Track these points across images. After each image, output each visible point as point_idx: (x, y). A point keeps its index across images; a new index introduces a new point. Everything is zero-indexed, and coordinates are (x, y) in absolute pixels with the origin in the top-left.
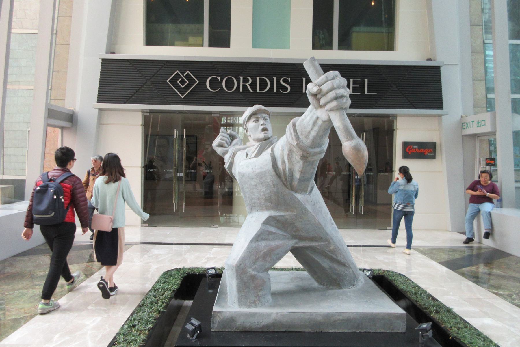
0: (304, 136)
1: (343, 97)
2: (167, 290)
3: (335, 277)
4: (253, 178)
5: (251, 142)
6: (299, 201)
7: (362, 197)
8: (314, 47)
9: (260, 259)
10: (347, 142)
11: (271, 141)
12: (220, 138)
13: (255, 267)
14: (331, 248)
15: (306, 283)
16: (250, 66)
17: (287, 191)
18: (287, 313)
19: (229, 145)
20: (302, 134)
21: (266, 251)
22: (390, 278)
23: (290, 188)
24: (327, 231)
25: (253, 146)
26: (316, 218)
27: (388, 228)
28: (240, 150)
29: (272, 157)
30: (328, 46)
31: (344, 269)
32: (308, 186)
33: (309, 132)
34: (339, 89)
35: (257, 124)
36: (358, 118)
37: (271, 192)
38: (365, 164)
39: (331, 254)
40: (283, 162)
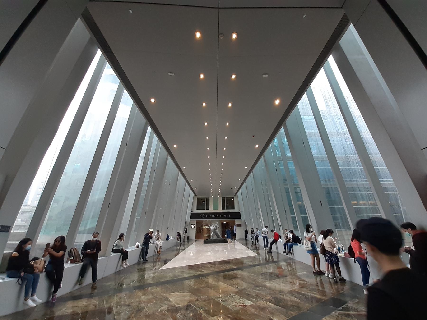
8: (222, 209)
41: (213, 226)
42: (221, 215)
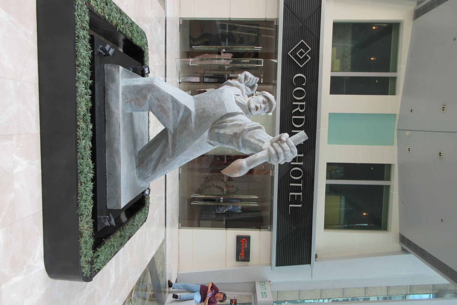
0: (251, 134)
1: (278, 159)
2: (132, 34)
3: (145, 162)
4: (220, 99)
5: (248, 99)
6: (203, 133)
7: (205, 203)
9: (159, 103)
10: (245, 162)
11: (248, 113)
12: (252, 77)
13: (153, 99)
14: (167, 159)
15: (139, 142)
16: (314, 111)
17: (210, 124)
18: (119, 121)
19: (246, 84)
20: (252, 133)
21: (165, 108)
22: (144, 210)
23: (213, 127)
24: (180, 156)
25: (245, 100)
26: (190, 147)
27: (180, 224)
28: (242, 92)
29: (236, 113)
30: (330, 176)
31: (151, 169)
32: (214, 140)
33: (253, 138)
34: (284, 156)
35: (261, 102)
36: (270, 200)
37: (209, 112)
38: (230, 174)
39: (162, 159)
40: (232, 121)
41: (248, 110)
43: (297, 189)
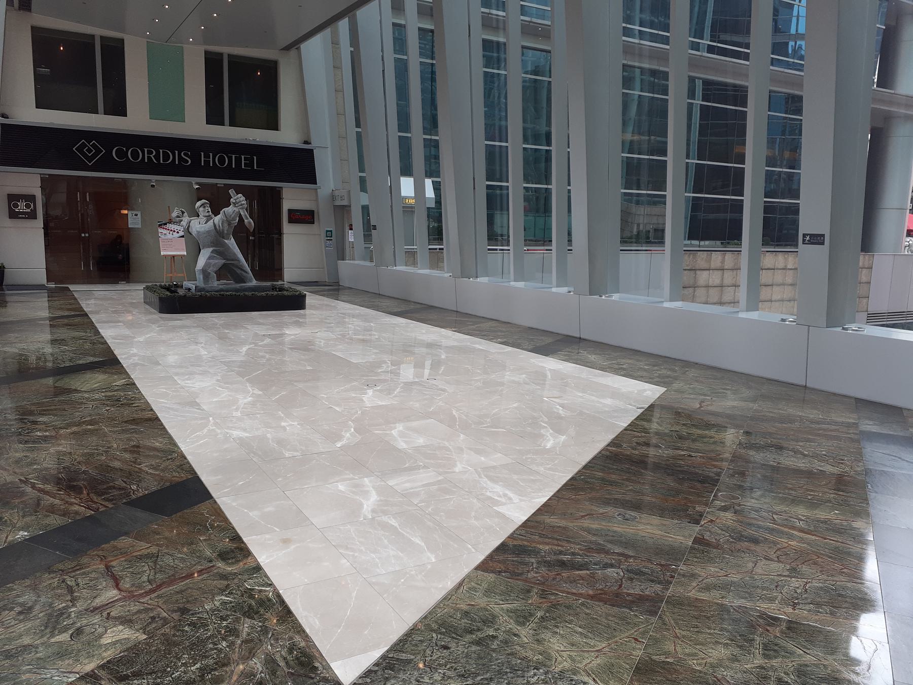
3: (243, 277)
8: (209, 122)
28: (192, 220)
33: (231, 215)
42: (207, 156)
43: (238, 161)
